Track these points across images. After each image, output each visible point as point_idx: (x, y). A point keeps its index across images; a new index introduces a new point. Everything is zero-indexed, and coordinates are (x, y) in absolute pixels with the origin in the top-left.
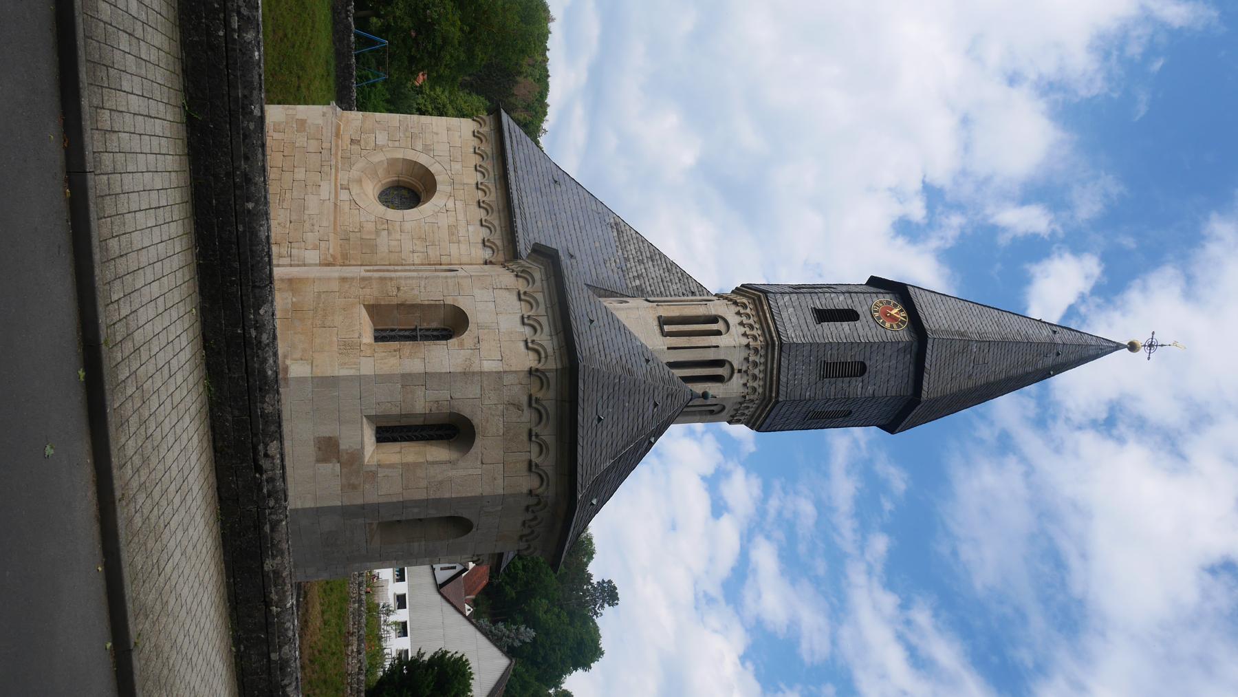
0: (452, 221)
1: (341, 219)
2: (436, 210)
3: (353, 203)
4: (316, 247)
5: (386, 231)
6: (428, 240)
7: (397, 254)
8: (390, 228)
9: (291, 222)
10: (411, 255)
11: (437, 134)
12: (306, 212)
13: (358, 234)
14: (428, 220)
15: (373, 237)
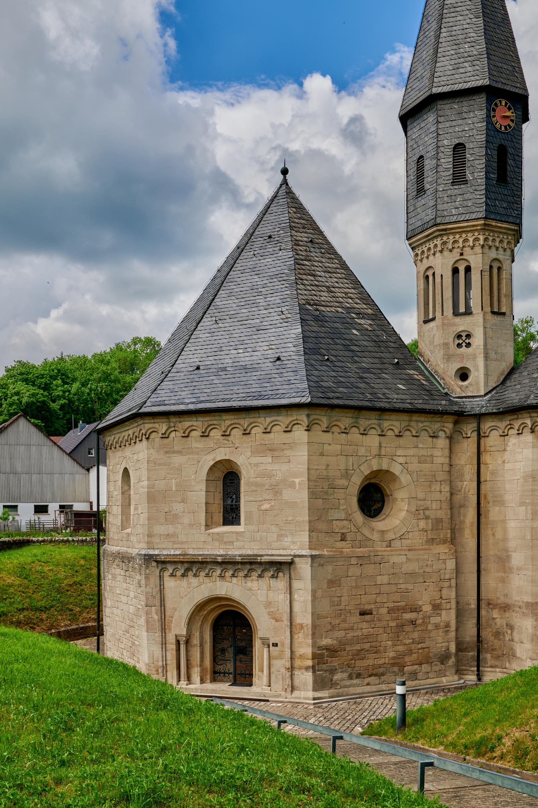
0: (415, 460)
1: (417, 545)
2: (406, 471)
3: (401, 537)
4: (444, 561)
5: (426, 511)
6: (431, 480)
7: (443, 504)
8: (422, 508)
9: (425, 582)
10: (443, 493)
11: (328, 465)
12: (417, 571)
13: (429, 532)
14: (415, 479)
15: (430, 521)
